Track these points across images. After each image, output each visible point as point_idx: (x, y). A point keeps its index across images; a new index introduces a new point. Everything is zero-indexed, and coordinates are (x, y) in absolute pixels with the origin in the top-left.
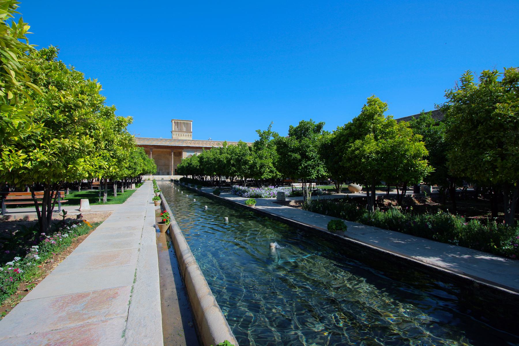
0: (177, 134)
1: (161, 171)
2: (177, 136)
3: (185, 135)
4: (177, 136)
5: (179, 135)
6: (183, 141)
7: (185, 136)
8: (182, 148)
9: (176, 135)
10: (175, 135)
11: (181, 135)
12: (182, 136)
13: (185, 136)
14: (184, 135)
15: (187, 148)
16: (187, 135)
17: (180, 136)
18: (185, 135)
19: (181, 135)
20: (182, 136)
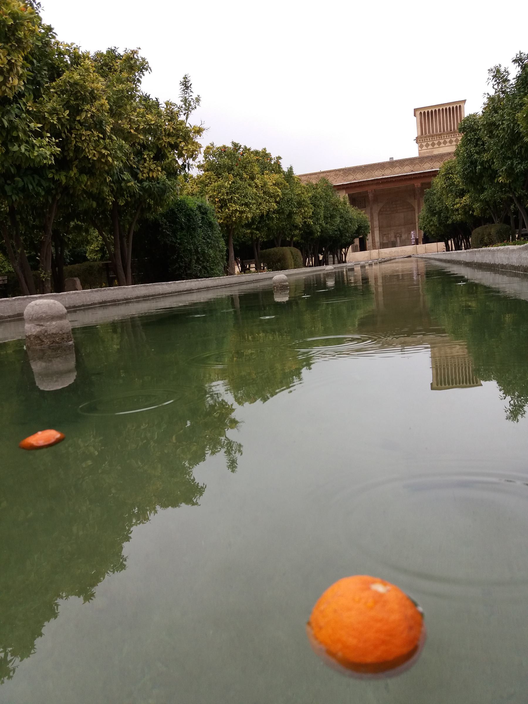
0: (430, 143)
1: (398, 239)
2: (430, 147)
3: (448, 140)
4: (430, 147)
5: (433, 145)
7: (448, 144)
9: (427, 145)
10: (424, 148)
12: (442, 145)
13: (448, 144)
14: (445, 143)
18: (448, 140)
19: (439, 144)
20: (442, 145)
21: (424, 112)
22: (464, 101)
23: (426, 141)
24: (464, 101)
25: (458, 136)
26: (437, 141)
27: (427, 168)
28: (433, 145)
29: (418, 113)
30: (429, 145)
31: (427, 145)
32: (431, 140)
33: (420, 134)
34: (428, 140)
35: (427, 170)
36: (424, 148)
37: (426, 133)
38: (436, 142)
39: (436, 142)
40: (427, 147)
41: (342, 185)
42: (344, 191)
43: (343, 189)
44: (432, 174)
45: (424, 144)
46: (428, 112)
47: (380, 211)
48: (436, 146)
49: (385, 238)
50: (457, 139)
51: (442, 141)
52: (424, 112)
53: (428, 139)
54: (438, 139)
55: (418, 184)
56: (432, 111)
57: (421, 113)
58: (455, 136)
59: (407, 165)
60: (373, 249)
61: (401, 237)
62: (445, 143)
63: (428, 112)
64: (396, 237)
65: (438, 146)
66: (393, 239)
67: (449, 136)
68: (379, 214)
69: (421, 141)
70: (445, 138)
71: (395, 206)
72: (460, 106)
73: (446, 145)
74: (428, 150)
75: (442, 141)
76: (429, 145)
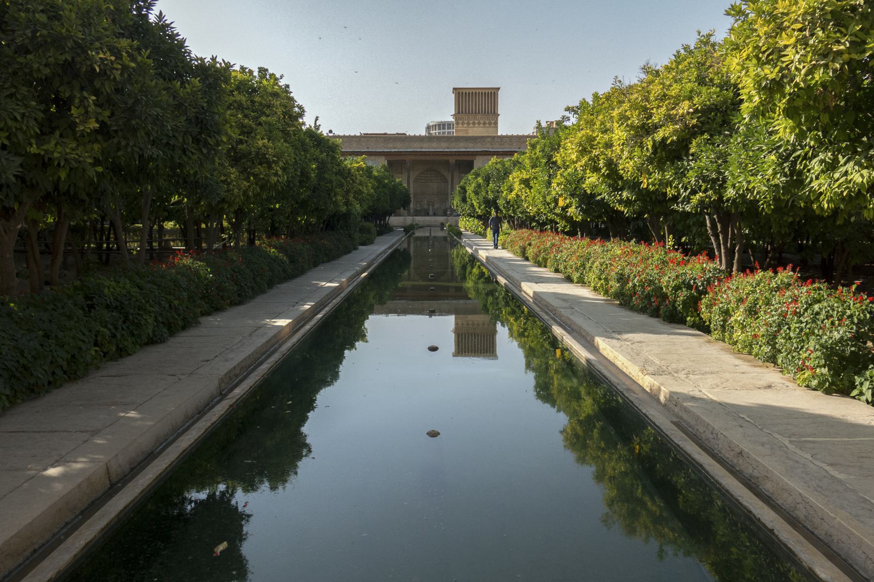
0: (466, 122)
1: (431, 207)
2: (466, 125)
3: (482, 122)
4: (466, 125)
5: (468, 124)
6: (474, 139)
8: (473, 155)
9: (463, 124)
11: (474, 123)
12: (476, 125)
13: (481, 125)
14: (479, 123)
15: (484, 155)
16: (487, 122)
17: (471, 125)
18: (482, 122)
19: (474, 123)
20: (476, 125)
22: (499, 89)
24: (499, 89)
26: (472, 121)
27: (462, 148)
28: (468, 124)
30: (464, 123)
31: (463, 124)
33: (457, 112)
36: (460, 125)
37: (462, 112)
38: (471, 122)
39: (471, 122)
41: (383, 152)
42: (384, 157)
43: (383, 155)
44: (466, 153)
45: (460, 122)
47: (416, 179)
48: (471, 125)
49: (418, 205)
50: (490, 122)
51: (476, 122)
55: (452, 160)
59: (444, 141)
60: (408, 216)
61: (434, 205)
62: (479, 123)
64: (428, 205)
66: (426, 207)
68: (414, 181)
71: (429, 175)
75: (476, 122)
76: (464, 123)
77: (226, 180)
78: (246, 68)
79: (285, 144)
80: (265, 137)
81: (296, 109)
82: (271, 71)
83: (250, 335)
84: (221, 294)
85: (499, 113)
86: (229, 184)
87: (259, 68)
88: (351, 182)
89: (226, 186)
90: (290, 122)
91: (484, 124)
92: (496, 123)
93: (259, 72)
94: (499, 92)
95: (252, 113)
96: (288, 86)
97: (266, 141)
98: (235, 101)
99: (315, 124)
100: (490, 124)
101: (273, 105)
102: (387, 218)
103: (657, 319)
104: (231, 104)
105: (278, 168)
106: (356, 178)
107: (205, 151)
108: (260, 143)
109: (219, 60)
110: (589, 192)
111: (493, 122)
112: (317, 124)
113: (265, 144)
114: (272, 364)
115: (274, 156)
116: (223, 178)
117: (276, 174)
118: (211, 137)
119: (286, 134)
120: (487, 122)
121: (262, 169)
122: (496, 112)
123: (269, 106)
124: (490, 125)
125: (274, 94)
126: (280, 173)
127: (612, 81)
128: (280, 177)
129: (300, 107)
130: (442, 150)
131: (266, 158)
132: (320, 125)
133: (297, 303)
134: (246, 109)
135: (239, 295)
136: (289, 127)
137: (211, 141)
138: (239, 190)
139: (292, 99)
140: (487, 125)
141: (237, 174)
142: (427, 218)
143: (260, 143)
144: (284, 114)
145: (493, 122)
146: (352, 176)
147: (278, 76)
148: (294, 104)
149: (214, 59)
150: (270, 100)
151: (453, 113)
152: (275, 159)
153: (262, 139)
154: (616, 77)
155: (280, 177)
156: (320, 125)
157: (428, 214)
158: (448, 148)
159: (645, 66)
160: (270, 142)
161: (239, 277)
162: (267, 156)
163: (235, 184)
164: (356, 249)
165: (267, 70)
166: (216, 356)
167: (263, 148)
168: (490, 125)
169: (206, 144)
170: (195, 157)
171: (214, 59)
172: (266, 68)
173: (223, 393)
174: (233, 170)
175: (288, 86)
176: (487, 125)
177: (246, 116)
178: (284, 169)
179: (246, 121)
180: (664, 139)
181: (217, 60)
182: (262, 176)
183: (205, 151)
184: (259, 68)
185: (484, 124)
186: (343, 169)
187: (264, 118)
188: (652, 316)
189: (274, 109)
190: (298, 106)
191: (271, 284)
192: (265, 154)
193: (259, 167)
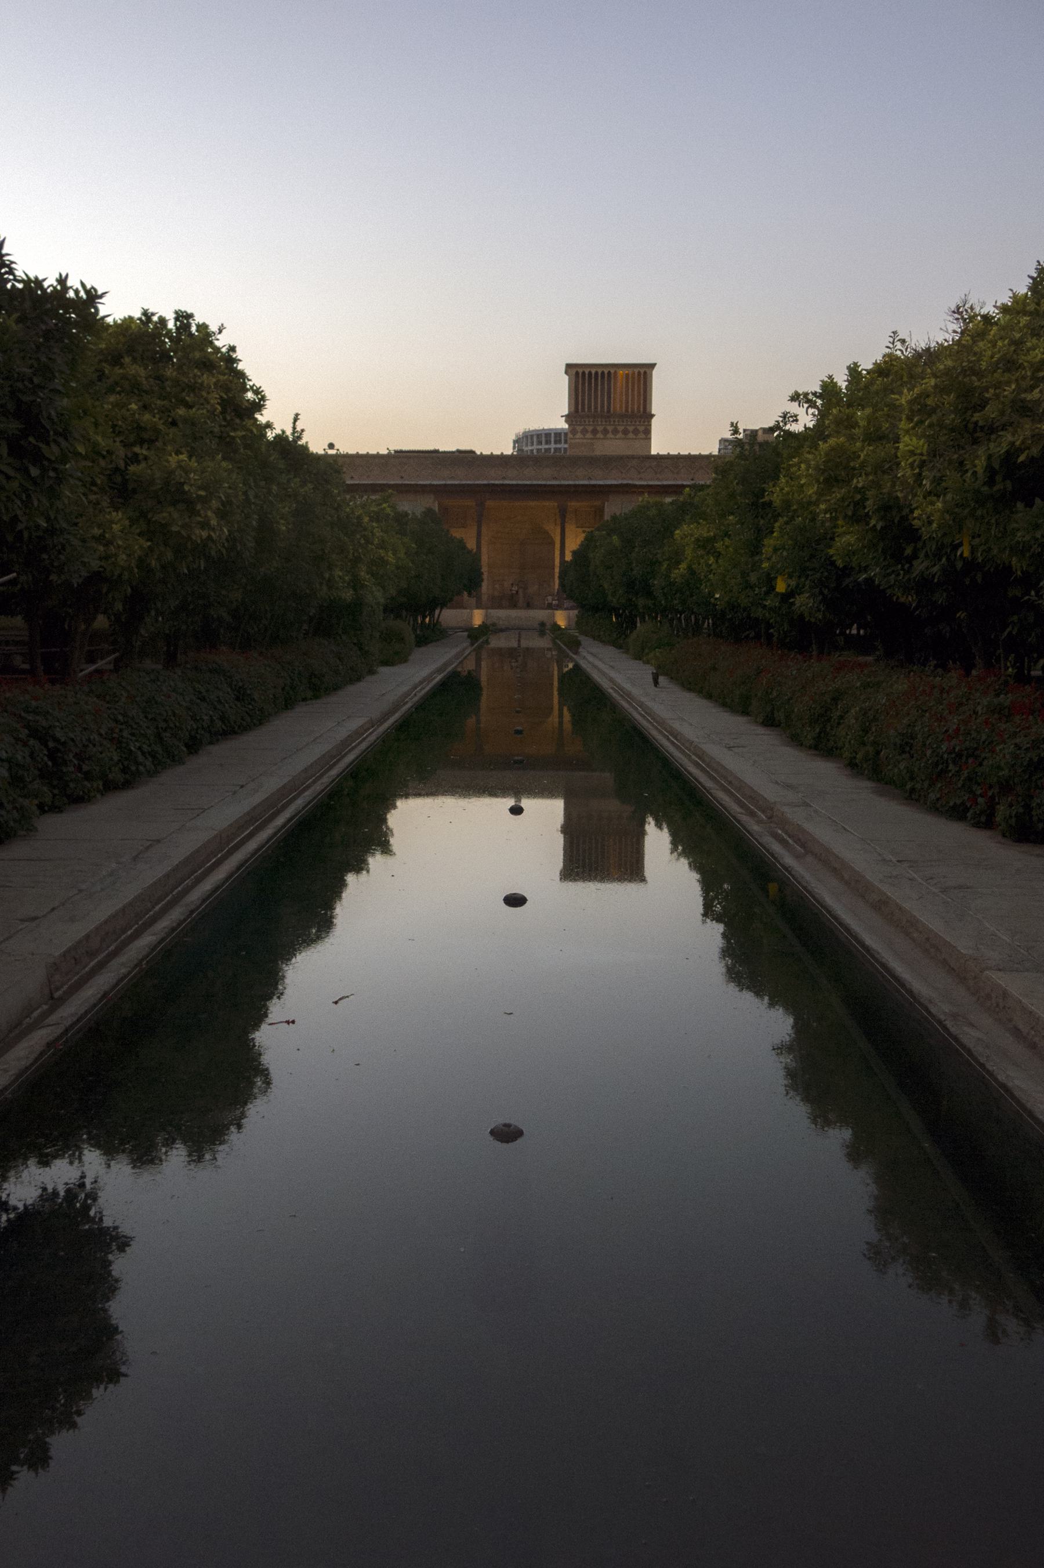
0: (590, 428)
2: (589, 435)
3: (620, 428)
5: (595, 432)
6: (607, 462)
7: (620, 435)
9: (584, 432)
10: (579, 435)
11: (605, 432)
12: (610, 435)
13: (620, 435)
16: (631, 428)
17: (600, 435)
18: (620, 428)
19: (605, 432)
20: (610, 435)
21: (584, 373)
22: (652, 366)
23: (583, 423)
24: (652, 366)
25: (638, 423)
28: (595, 432)
29: (574, 371)
30: (587, 431)
32: (591, 423)
33: (573, 409)
34: (587, 423)
35: (583, 480)
36: (579, 435)
39: (600, 428)
40: (584, 435)
45: (579, 428)
46: (590, 373)
48: (600, 435)
52: (584, 373)
53: (587, 420)
54: (604, 423)
56: (596, 373)
57: (577, 373)
58: (633, 423)
60: (478, 608)
62: (615, 432)
63: (590, 373)
65: (602, 436)
67: (623, 422)
69: (574, 423)
70: (617, 423)
72: (645, 373)
73: (617, 437)
74: (585, 441)
76: (587, 431)
77: (102, 536)
78: (153, 314)
79: (224, 464)
80: (183, 450)
81: (250, 395)
82: (199, 319)
83: (135, 859)
84: (85, 768)
85: (653, 412)
86: (108, 543)
87: (176, 312)
88: (363, 541)
89: (102, 548)
90: (238, 421)
91: (625, 432)
92: (648, 432)
93: (177, 319)
94: (655, 372)
95: (159, 402)
96: (232, 349)
97: (183, 457)
98: (124, 377)
99: (294, 428)
100: (636, 432)
101: (202, 384)
102: (437, 612)
103: (988, 833)
104: (117, 384)
105: (209, 513)
106: (373, 534)
107: (35, 472)
108: (173, 460)
109: (73, 282)
110: (840, 563)
111: (641, 428)
112: (298, 429)
113: (183, 464)
114: (163, 935)
115: (200, 488)
116: (96, 531)
117: (205, 525)
118: (48, 444)
119: (225, 442)
120: (631, 428)
121: (176, 515)
122: (648, 410)
123: (193, 388)
124: (636, 435)
125: (204, 364)
126: (214, 522)
127: (887, 341)
128: (213, 529)
129: (257, 392)
130: (543, 483)
131: (184, 492)
132: (303, 431)
133: (242, 787)
134: (146, 392)
135: (125, 770)
136: (235, 430)
137: (52, 451)
138: (129, 556)
139: (241, 375)
140: (631, 435)
141: (127, 523)
142: (513, 613)
143: (173, 460)
144: (224, 403)
145: (641, 428)
146: (365, 529)
147: (213, 328)
148: (245, 384)
149: (62, 281)
150: (195, 376)
151: (566, 412)
152: (202, 493)
153: (178, 453)
154: (894, 333)
155: (213, 529)
156: (303, 431)
157: (514, 606)
158: (555, 478)
159: (958, 308)
160: (194, 459)
161: (125, 734)
162: (186, 488)
163: (120, 543)
164: (372, 672)
165: (190, 316)
166: (53, 909)
167: (178, 472)
168: (636, 435)
169: (38, 458)
170: (15, 485)
171: (62, 281)
172: (189, 312)
173: (57, 995)
174: (117, 515)
175: (232, 349)
176: (631, 435)
177: (145, 407)
178: (223, 514)
179: (147, 416)
180: (1010, 456)
181: (69, 283)
182: (175, 529)
183: (35, 472)
184: (176, 312)
185: (625, 432)
186: (348, 517)
187: (181, 411)
188: (978, 825)
189: (204, 394)
190: (252, 387)
191: (193, 746)
192: (182, 484)
193: (171, 509)
